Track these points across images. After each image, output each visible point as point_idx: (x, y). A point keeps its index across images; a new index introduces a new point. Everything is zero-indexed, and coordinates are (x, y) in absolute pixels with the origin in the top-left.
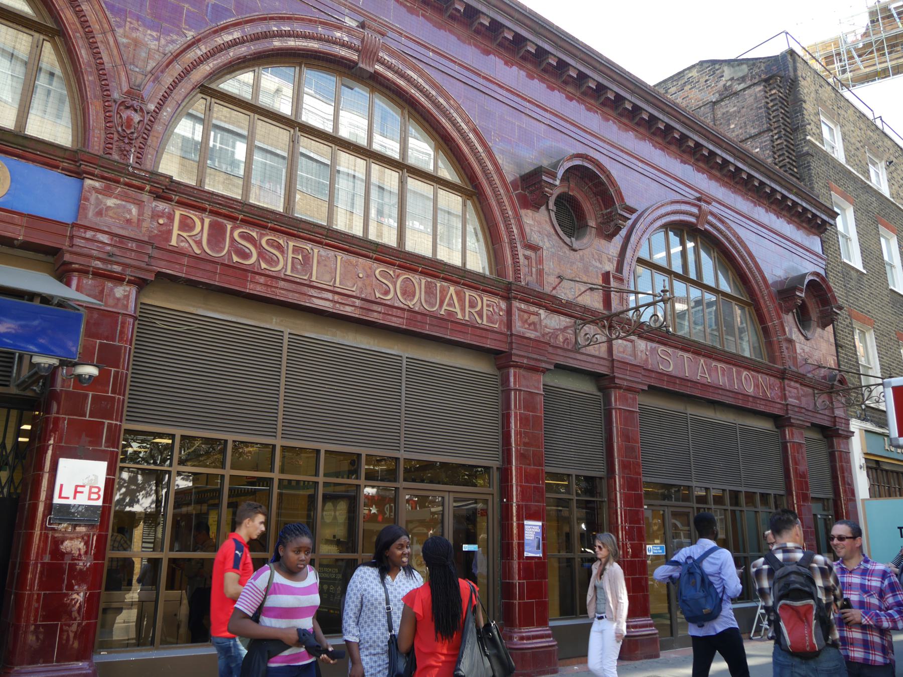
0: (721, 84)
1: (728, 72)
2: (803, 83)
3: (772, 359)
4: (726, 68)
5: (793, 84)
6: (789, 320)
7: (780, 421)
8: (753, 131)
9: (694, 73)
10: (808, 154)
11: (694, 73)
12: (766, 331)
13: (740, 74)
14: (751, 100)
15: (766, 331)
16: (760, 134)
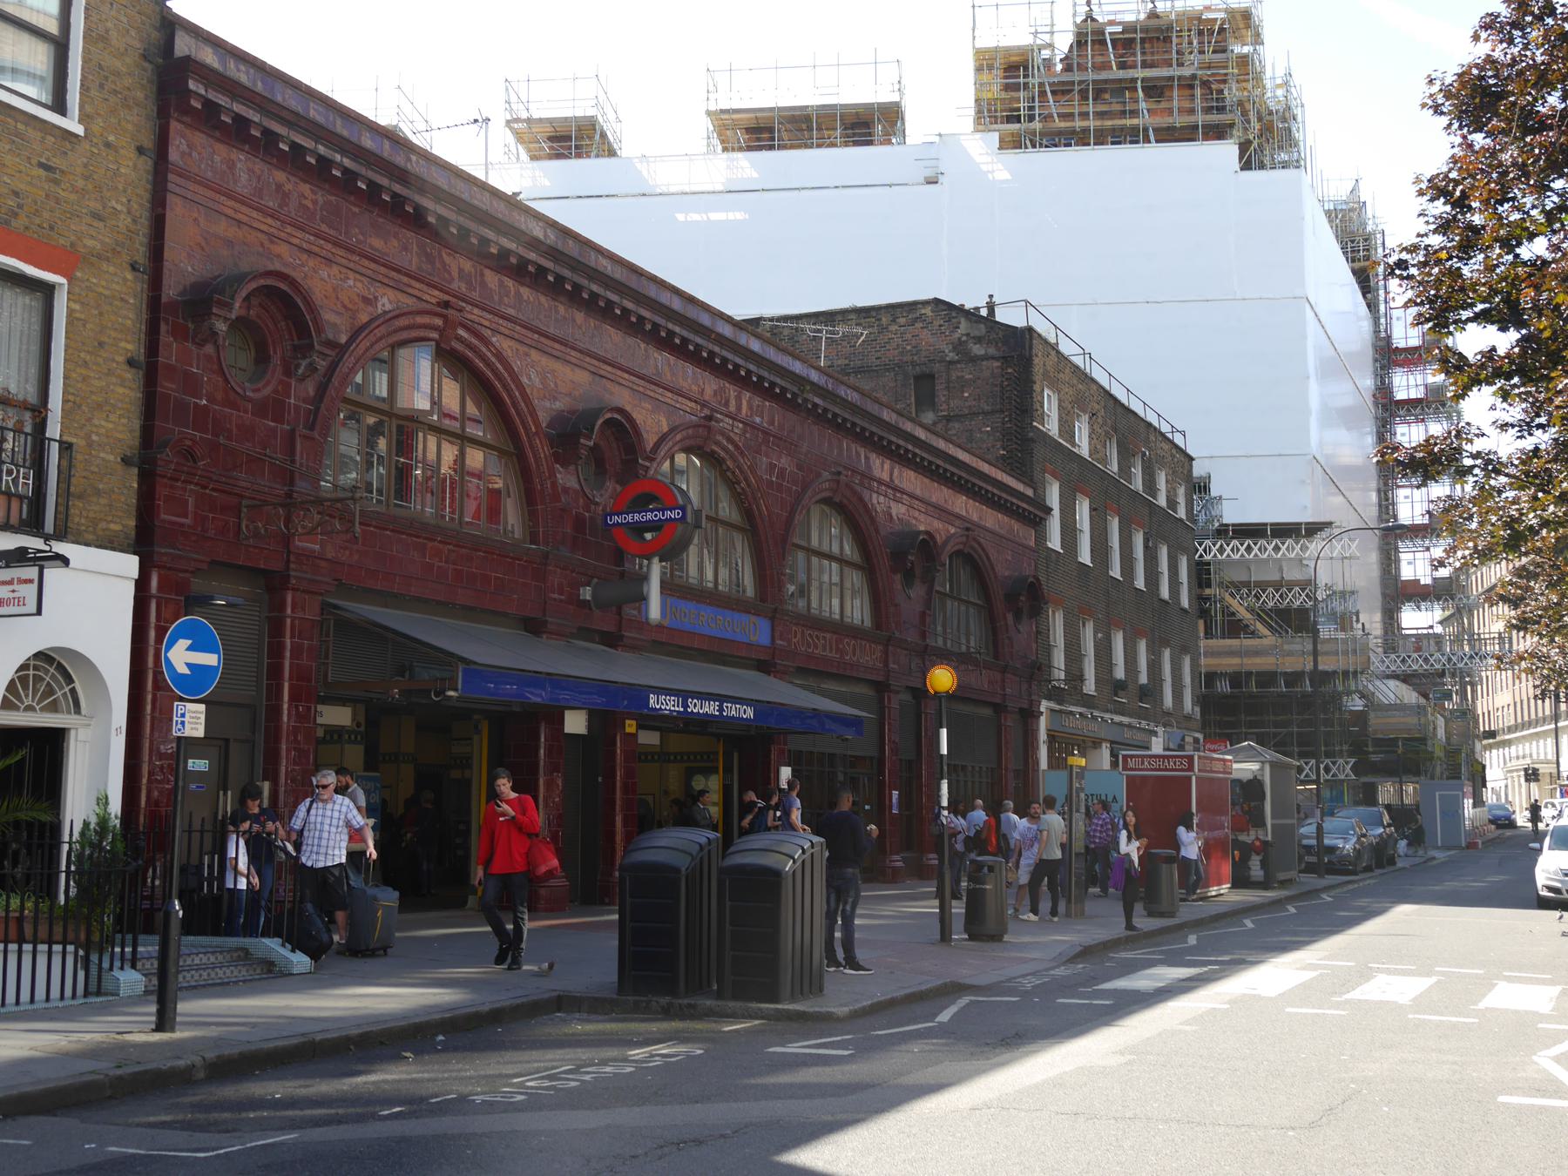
0: (957, 335)
1: (964, 326)
2: (1036, 361)
3: (996, 657)
4: (962, 320)
5: (1026, 363)
6: (1010, 617)
7: (999, 708)
8: (987, 408)
9: (928, 311)
10: (1032, 440)
11: (928, 311)
12: (995, 632)
13: (977, 333)
14: (987, 374)
15: (995, 632)
16: (993, 412)
